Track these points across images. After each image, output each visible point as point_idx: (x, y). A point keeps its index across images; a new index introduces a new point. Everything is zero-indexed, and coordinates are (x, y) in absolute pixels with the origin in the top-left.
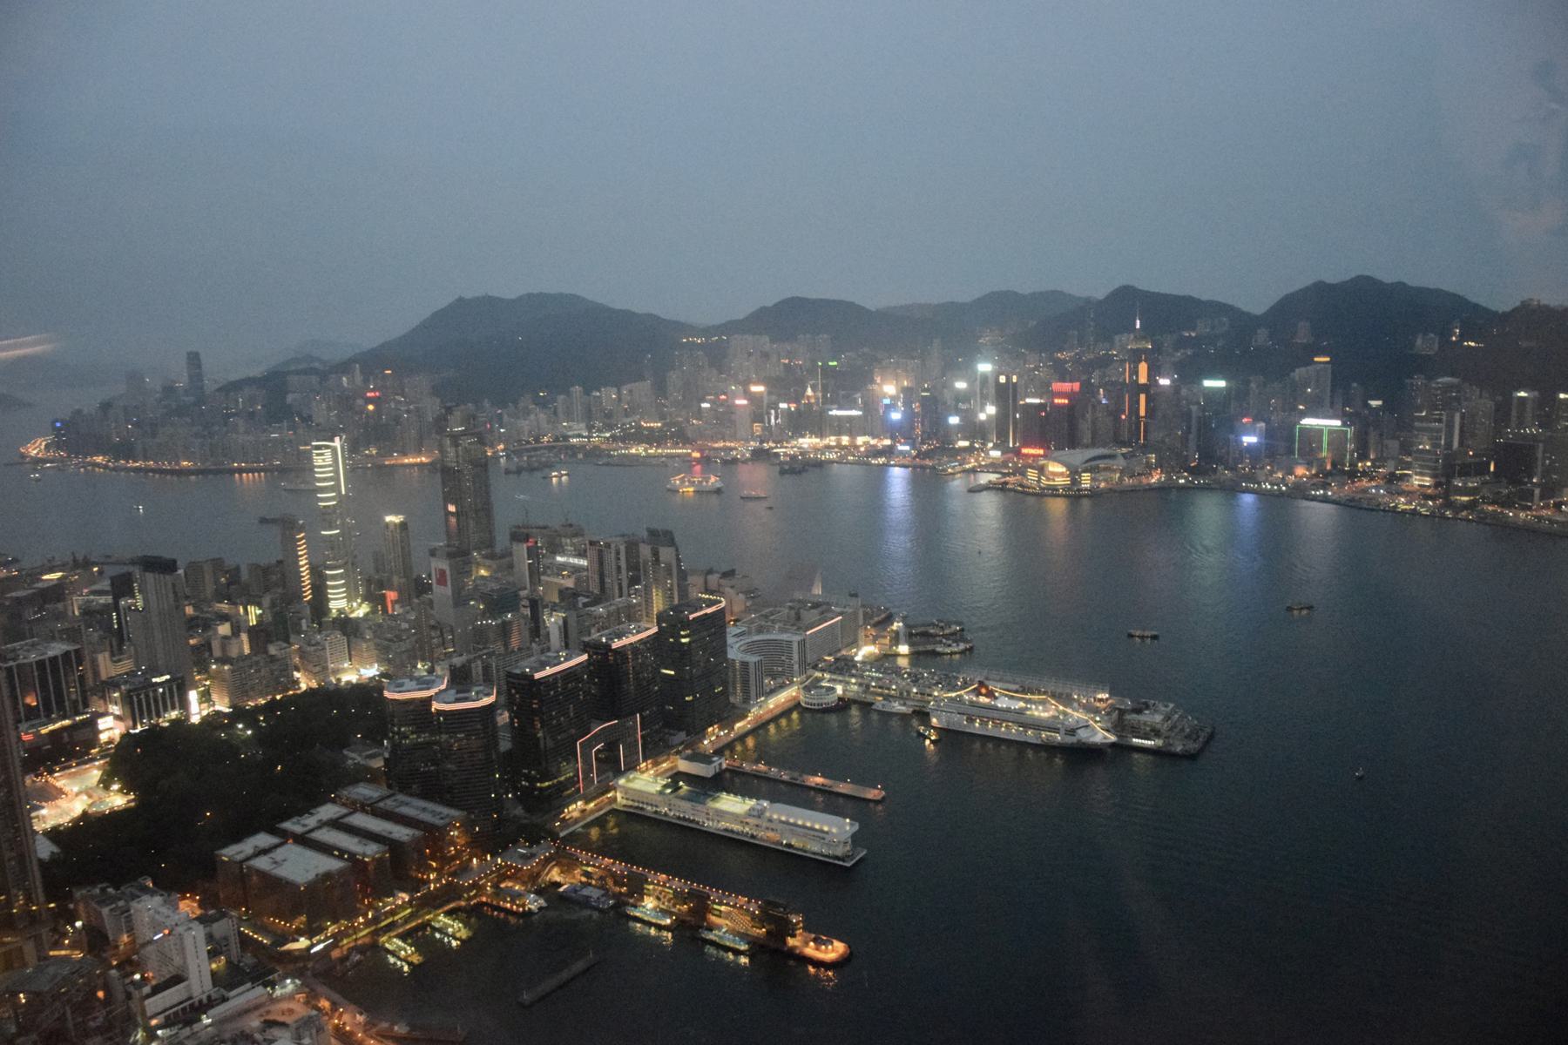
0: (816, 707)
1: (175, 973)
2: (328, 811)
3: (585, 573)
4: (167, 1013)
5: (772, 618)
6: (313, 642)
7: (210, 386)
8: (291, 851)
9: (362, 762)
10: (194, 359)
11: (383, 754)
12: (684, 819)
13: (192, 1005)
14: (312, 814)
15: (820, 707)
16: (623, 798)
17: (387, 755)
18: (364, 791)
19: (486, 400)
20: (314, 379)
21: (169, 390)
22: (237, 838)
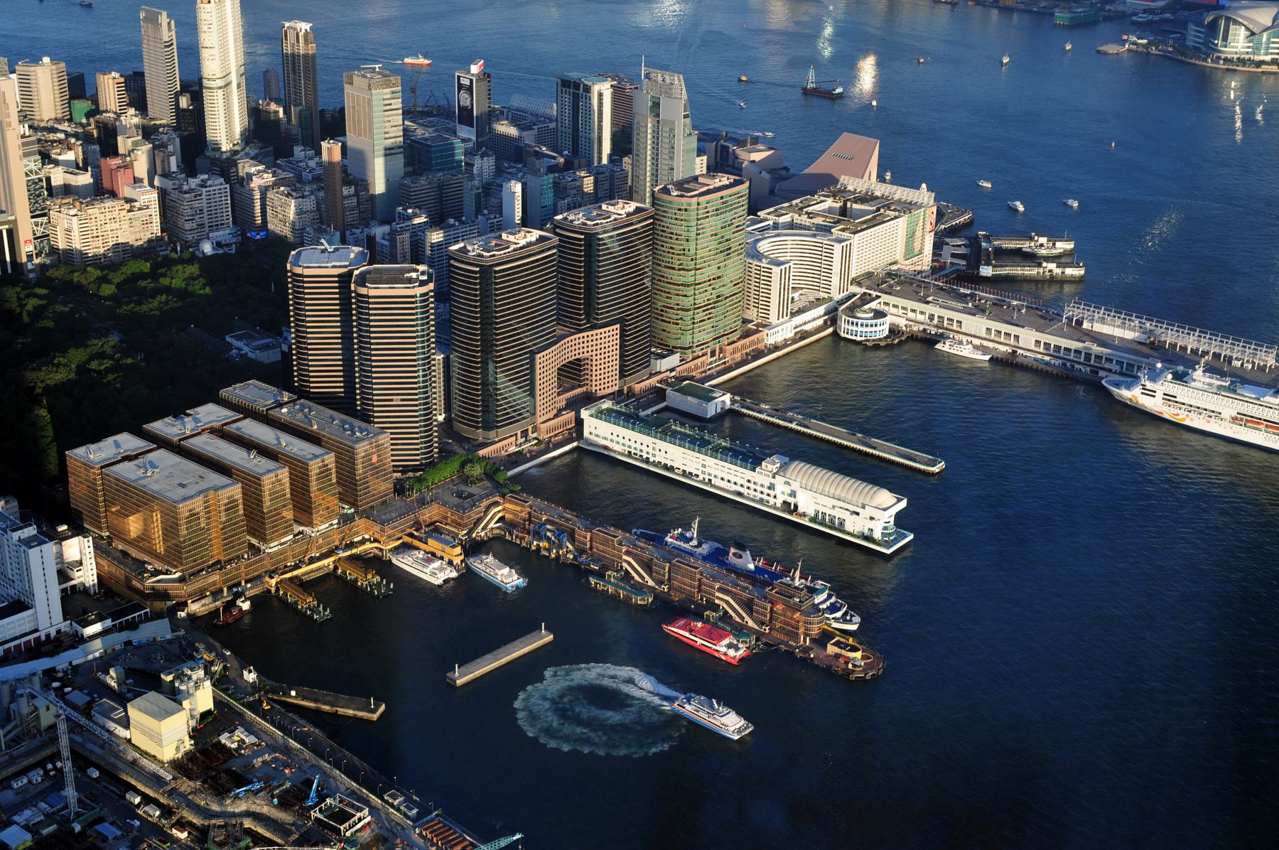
0: (859, 339)
1: (17, 598)
2: (210, 413)
3: (552, 125)
4: (6, 646)
5: (810, 209)
6: (185, 188)
8: (161, 456)
9: (251, 355)
11: (281, 347)
12: (671, 469)
13: (38, 639)
14: (189, 415)
15: (863, 338)
16: (591, 433)
17: (285, 348)
18: (253, 392)
22: (96, 439)
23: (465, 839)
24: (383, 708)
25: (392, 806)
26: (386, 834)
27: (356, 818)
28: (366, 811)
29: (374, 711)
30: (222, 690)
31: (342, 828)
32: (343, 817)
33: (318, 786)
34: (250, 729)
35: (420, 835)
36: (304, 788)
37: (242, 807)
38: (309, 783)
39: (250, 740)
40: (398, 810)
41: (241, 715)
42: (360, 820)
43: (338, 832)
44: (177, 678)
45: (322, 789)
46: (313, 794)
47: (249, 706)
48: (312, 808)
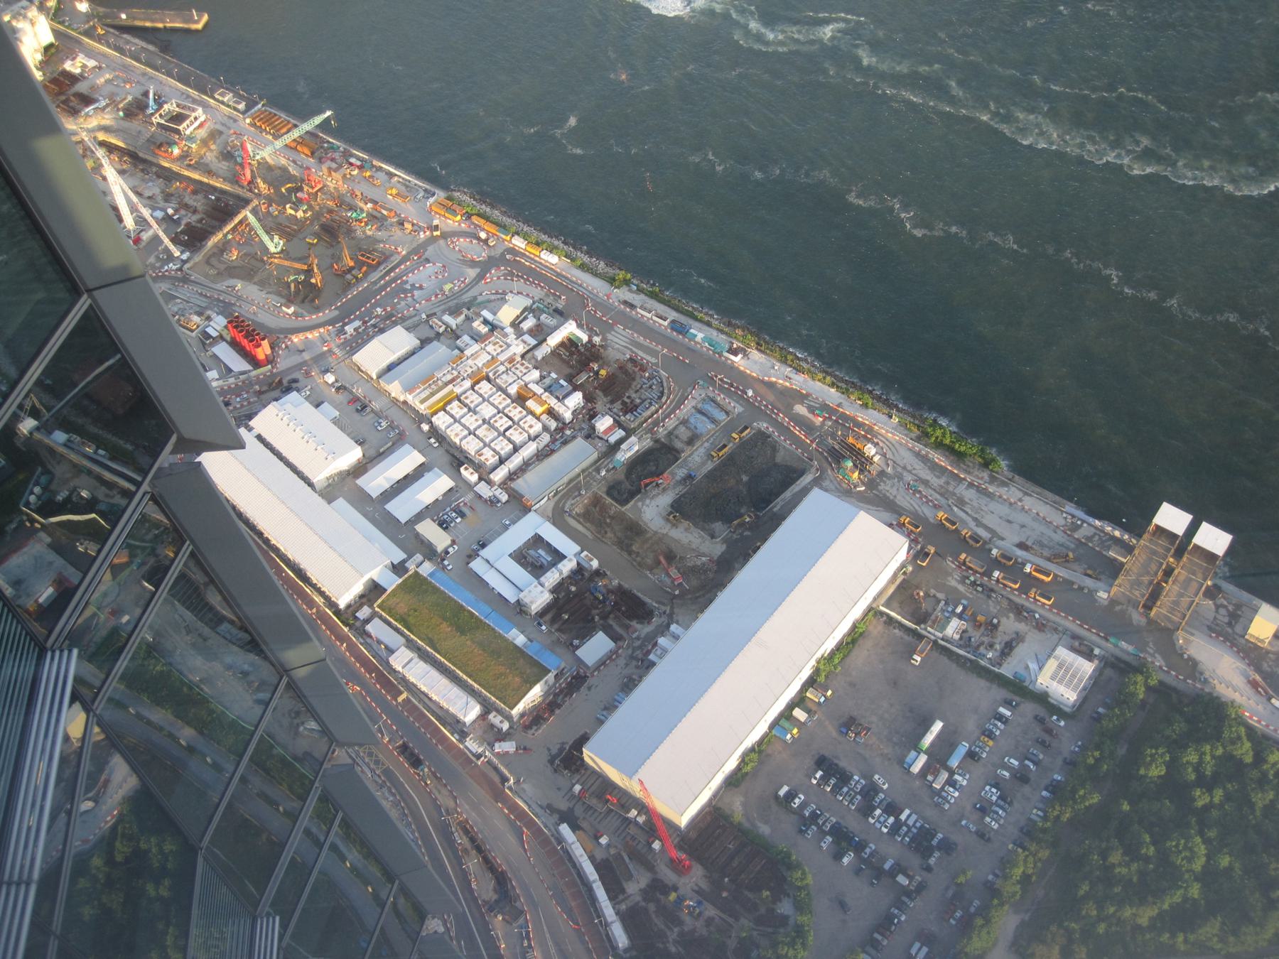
23: (289, 122)
24: (206, 18)
25: (223, 103)
26: (219, 127)
27: (192, 118)
28: (200, 110)
29: (197, 22)
30: (62, 23)
31: (181, 128)
32: (179, 118)
33: (155, 95)
34: (90, 54)
35: (251, 125)
36: (144, 99)
37: (93, 123)
38: (146, 94)
39: (91, 63)
40: (228, 106)
41: (79, 42)
42: (196, 119)
43: (178, 132)
44: (14, 17)
45: (159, 97)
46: (151, 102)
47: (89, 33)
48: (152, 114)
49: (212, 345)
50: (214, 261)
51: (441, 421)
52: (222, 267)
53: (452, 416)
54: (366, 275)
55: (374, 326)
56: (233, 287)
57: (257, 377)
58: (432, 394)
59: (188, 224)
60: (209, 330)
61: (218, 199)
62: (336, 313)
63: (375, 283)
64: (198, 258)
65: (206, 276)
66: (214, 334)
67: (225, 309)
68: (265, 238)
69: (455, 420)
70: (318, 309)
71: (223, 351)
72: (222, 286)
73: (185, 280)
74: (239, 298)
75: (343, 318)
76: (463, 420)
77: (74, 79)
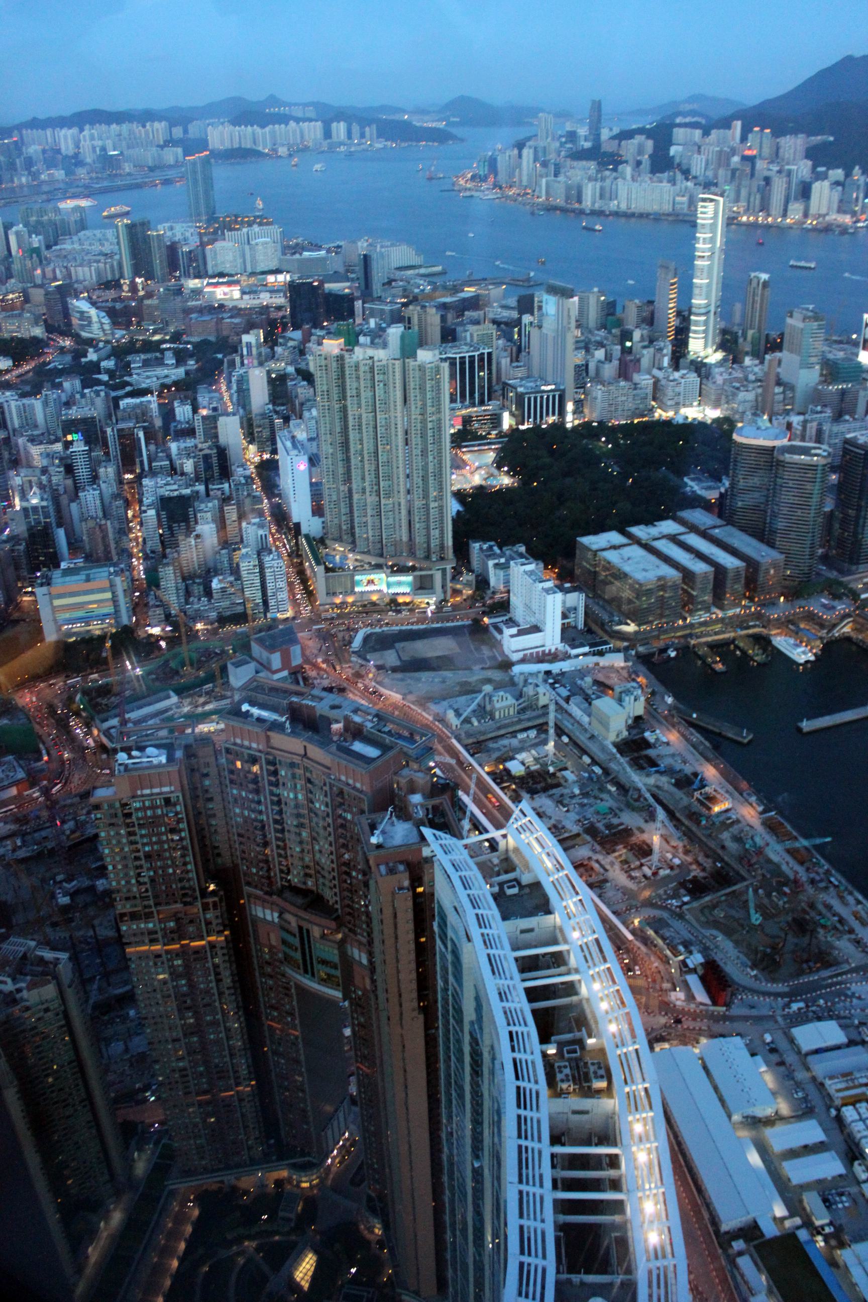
7: (605, 134)
10: (597, 107)
19: (857, 168)
20: (698, 133)
21: (572, 136)
49: (686, 972)
50: (706, 911)
51: (849, 1113)
52: (711, 918)
53: (859, 1114)
54: (818, 970)
55: (814, 1012)
56: (715, 938)
57: (713, 1012)
58: (847, 1089)
59: (695, 877)
60: (688, 961)
61: (722, 867)
62: (787, 989)
63: (824, 979)
64: (695, 904)
65: (698, 920)
66: (691, 966)
67: (705, 951)
68: (752, 911)
69: (861, 1119)
70: (773, 980)
71: (693, 981)
72: (708, 932)
73: (681, 916)
74: (717, 947)
75: (792, 995)
76: (857, 1117)
77: (647, 745)
